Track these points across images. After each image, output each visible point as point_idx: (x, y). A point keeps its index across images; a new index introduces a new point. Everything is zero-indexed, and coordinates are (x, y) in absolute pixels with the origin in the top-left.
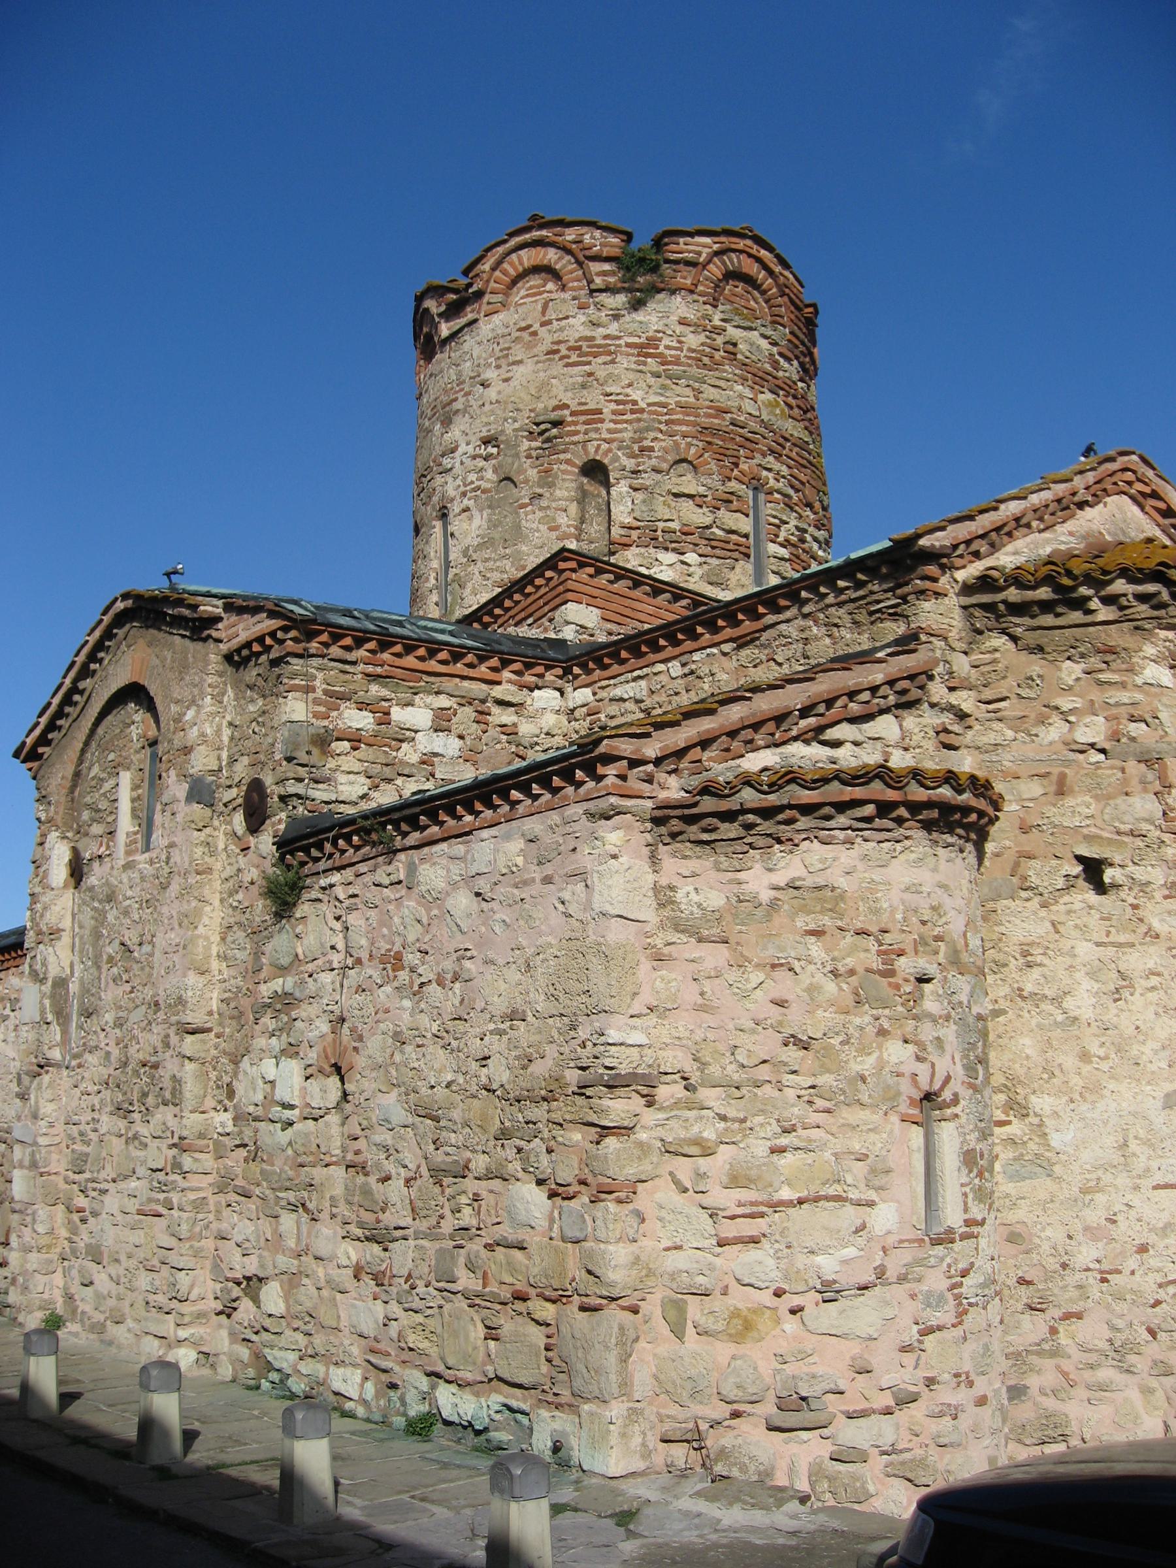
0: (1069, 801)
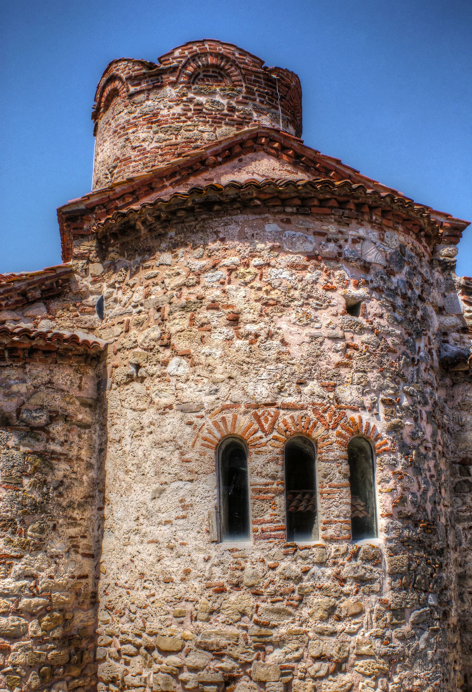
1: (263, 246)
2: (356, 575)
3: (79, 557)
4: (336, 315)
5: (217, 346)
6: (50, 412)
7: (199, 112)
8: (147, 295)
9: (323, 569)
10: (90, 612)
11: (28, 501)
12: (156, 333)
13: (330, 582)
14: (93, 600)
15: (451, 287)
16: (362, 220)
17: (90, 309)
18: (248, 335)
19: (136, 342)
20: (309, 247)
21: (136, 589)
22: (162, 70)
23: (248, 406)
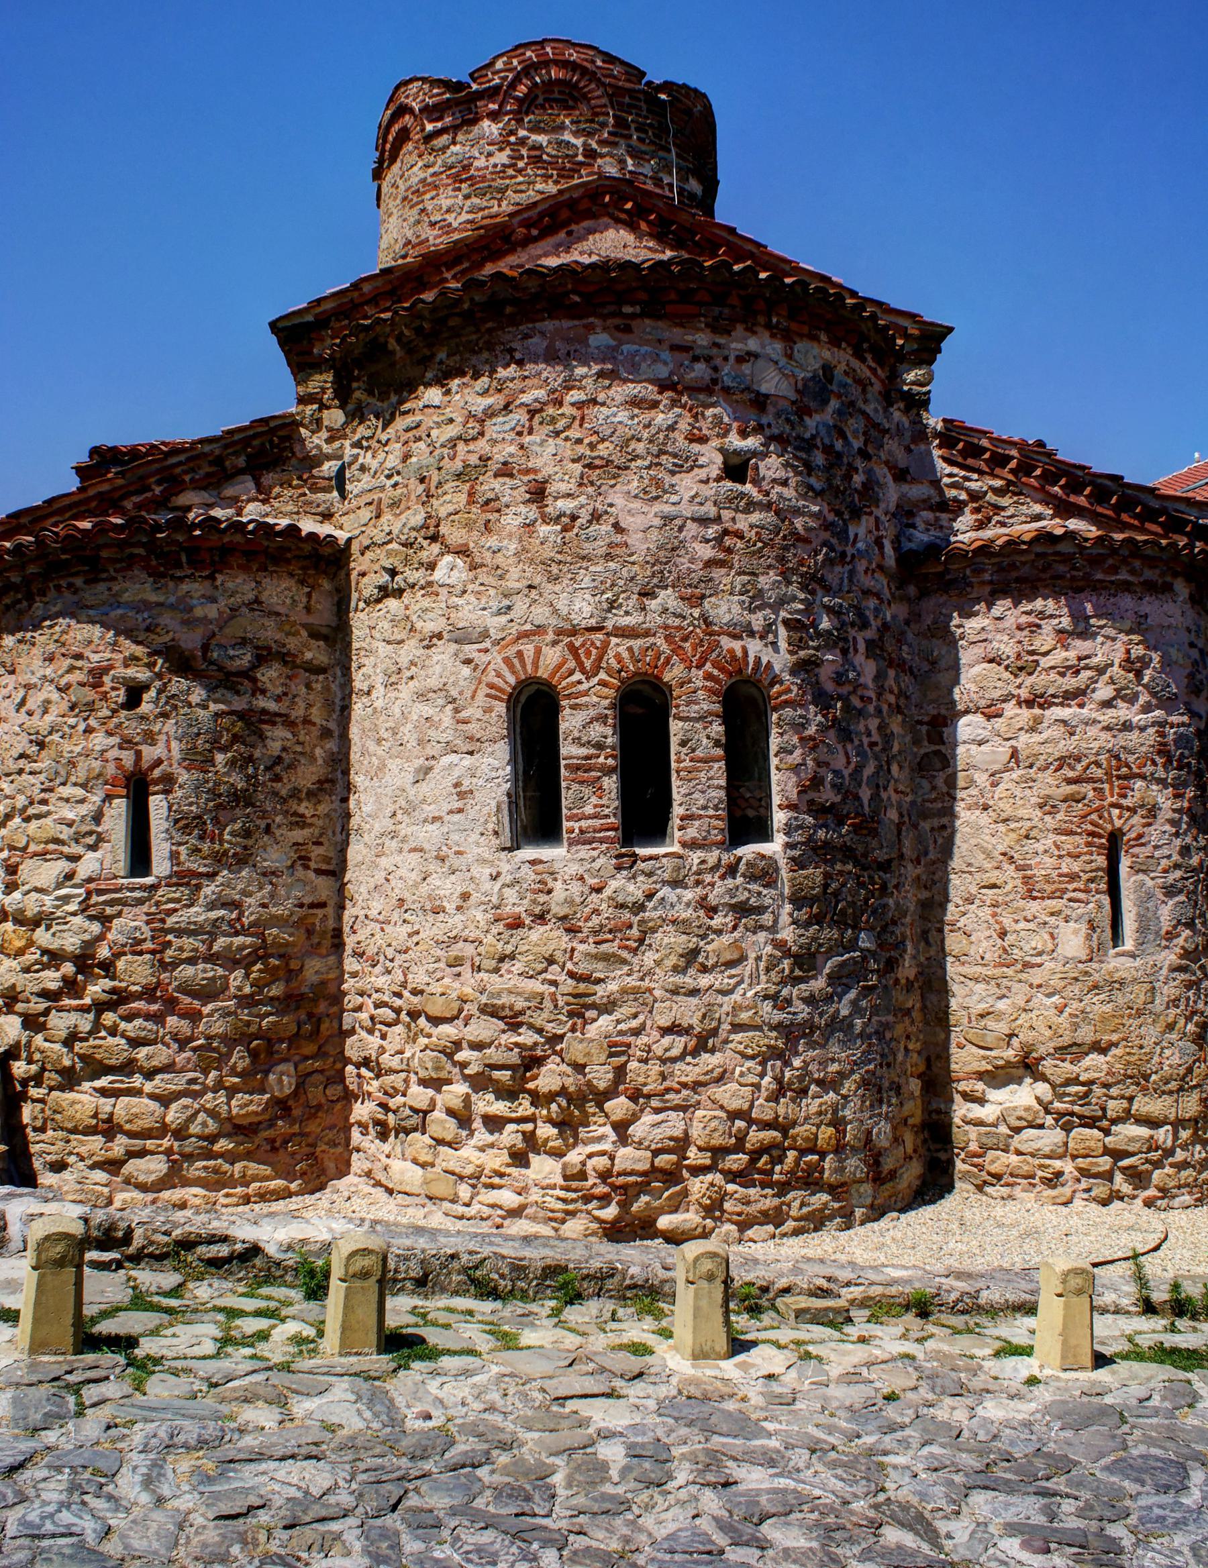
1: (585, 370)
2: (734, 901)
3: (311, 875)
4: (706, 482)
5: (510, 535)
6: (257, 648)
7: (536, 160)
8: (406, 457)
9: (678, 891)
10: (332, 959)
11: (223, 788)
12: (418, 519)
13: (690, 911)
14: (336, 941)
15: (921, 434)
16: (754, 325)
17: (325, 483)
18: (559, 516)
19: (389, 533)
20: (663, 372)
22: (477, 92)
23: (559, 632)
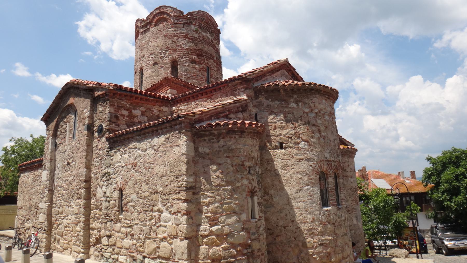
0: (276, 130)
12: (293, 132)
21: (289, 226)
23: (326, 161)
